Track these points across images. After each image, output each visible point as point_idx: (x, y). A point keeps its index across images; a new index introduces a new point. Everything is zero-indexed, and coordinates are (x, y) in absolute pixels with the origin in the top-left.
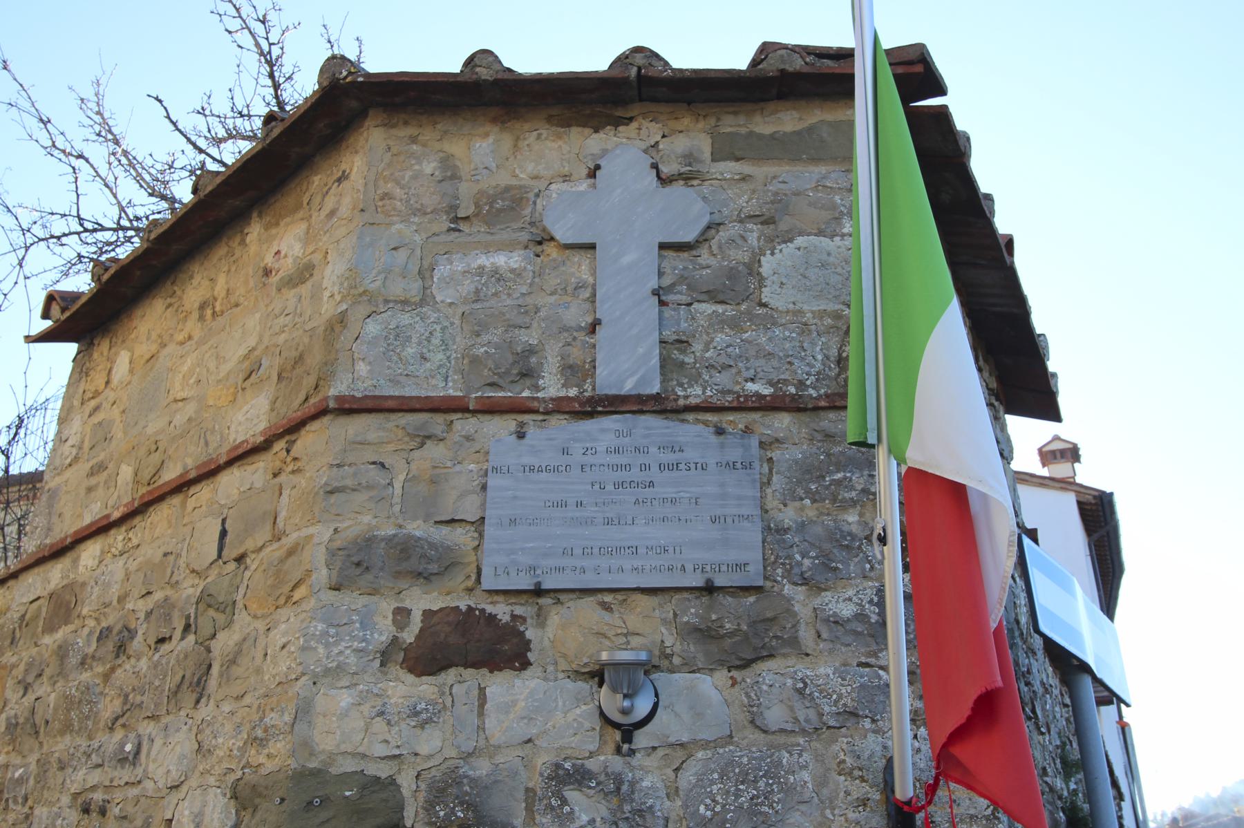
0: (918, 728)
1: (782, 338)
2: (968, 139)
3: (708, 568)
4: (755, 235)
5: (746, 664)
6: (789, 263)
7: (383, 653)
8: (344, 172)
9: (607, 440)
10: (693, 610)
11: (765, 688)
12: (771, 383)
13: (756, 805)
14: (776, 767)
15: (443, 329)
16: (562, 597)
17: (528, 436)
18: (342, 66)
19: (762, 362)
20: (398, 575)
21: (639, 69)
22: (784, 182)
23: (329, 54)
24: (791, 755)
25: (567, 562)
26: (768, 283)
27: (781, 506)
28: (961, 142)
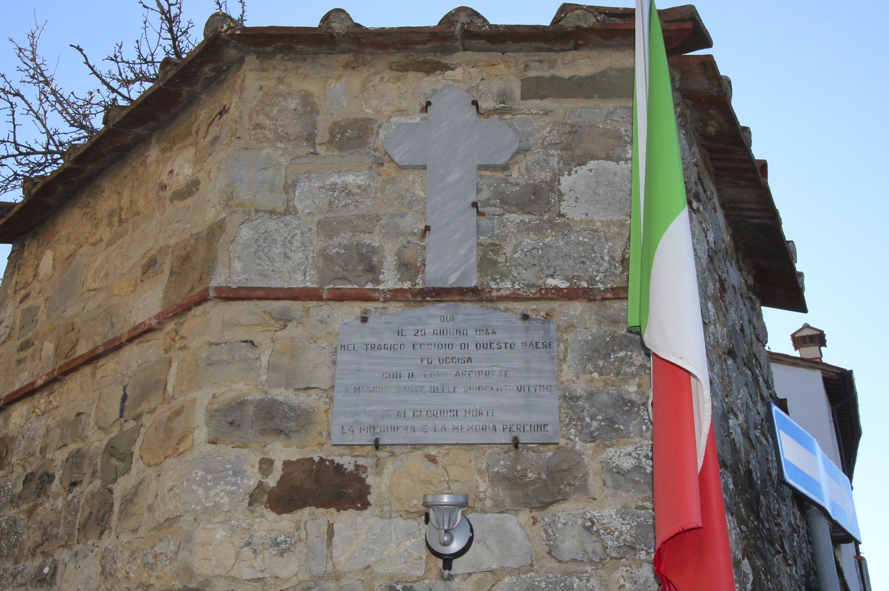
2: (730, 83)
3: (515, 428)
4: (556, 159)
5: (545, 506)
6: (583, 182)
7: (251, 496)
8: (225, 107)
9: (435, 324)
10: (502, 462)
11: (560, 525)
12: (567, 279)
15: (303, 234)
16: (397, 450)
17: (370, 320)
18: (223, 21)
20: (263, 432)
23: (214, 12)
24: (581, 580)
25: (401, 422)
26: (566, 197)
27: (575, 378)
28: (725, 84)
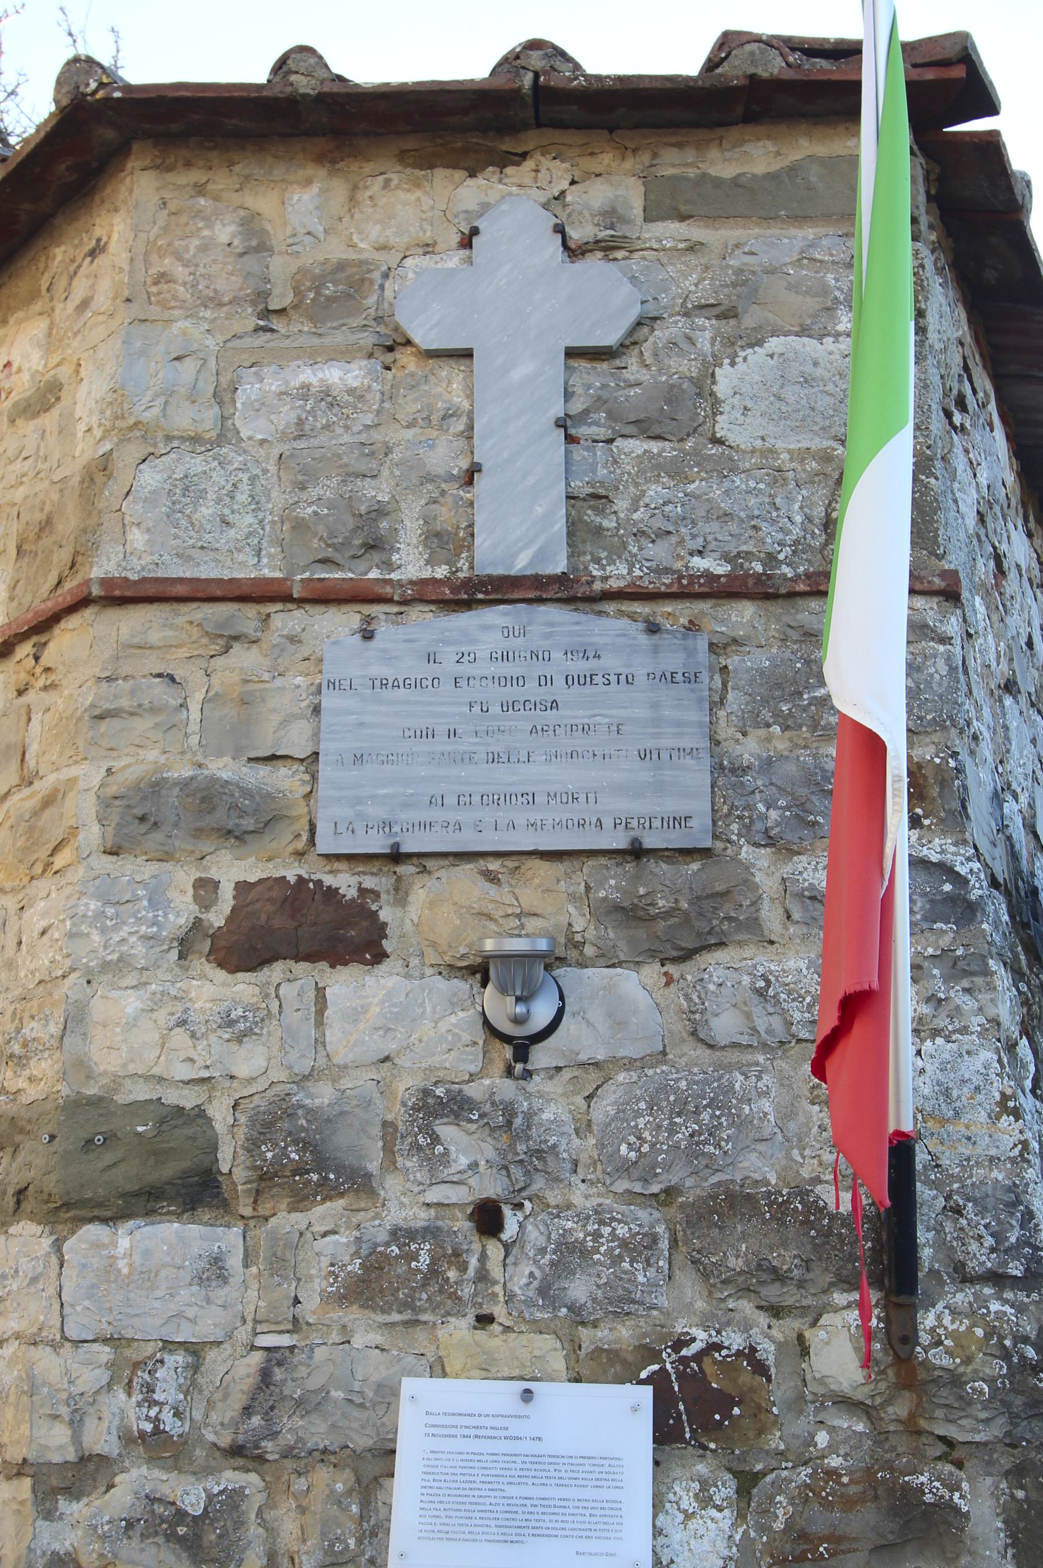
0: (922, 1041)
1: (744, 491)
2: (1028, 184)
3: (634, 823)
4: (708, 334)
5: (686, 956)
6: (757, 378)
7: (182, 942)
8: (99, 240)
9: (492, 642)
10: (612, 882)
11: (712, 987)
12: (726, 558)
13: (697, 1144)
14: (725, 1094)
15: (253, 479)
16: (430, 864)
17: (378, 636)
18: (88, 73)
19: (715, 526)
20: (198, 833)
21: (537, 75)
22: (753, 254)
23: (70, 54)
24: (747, 1077)
25: (436, 815)
26: (725, 408)
27: (739, 736)
28: (1018, 189)
